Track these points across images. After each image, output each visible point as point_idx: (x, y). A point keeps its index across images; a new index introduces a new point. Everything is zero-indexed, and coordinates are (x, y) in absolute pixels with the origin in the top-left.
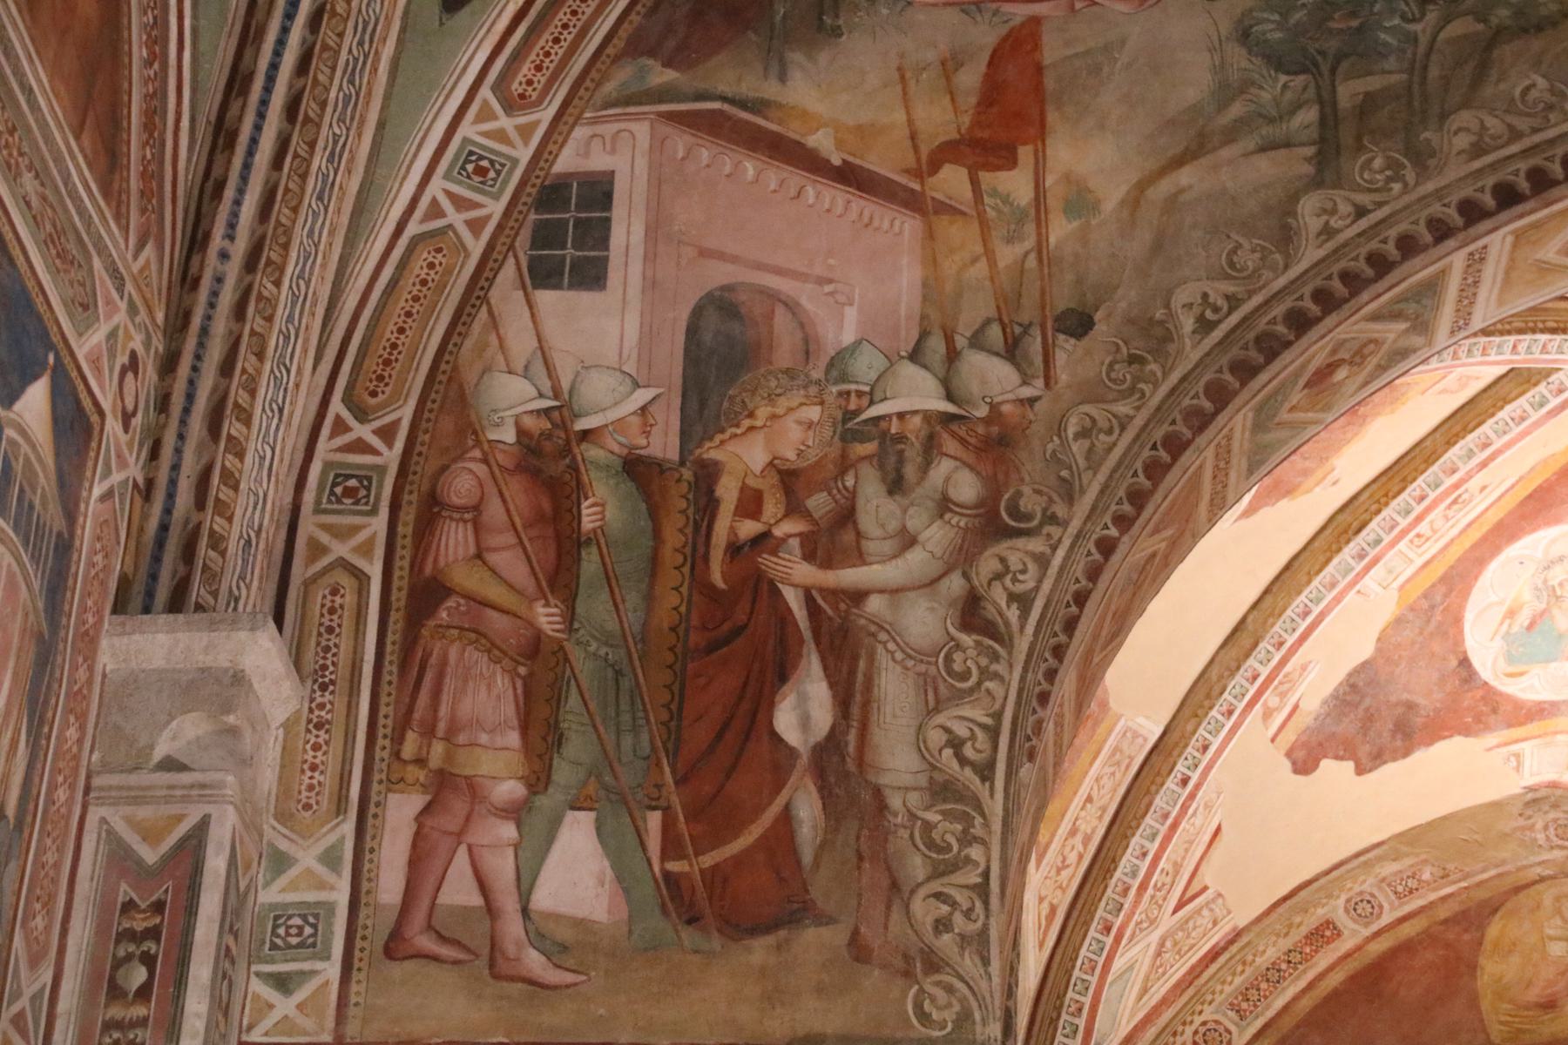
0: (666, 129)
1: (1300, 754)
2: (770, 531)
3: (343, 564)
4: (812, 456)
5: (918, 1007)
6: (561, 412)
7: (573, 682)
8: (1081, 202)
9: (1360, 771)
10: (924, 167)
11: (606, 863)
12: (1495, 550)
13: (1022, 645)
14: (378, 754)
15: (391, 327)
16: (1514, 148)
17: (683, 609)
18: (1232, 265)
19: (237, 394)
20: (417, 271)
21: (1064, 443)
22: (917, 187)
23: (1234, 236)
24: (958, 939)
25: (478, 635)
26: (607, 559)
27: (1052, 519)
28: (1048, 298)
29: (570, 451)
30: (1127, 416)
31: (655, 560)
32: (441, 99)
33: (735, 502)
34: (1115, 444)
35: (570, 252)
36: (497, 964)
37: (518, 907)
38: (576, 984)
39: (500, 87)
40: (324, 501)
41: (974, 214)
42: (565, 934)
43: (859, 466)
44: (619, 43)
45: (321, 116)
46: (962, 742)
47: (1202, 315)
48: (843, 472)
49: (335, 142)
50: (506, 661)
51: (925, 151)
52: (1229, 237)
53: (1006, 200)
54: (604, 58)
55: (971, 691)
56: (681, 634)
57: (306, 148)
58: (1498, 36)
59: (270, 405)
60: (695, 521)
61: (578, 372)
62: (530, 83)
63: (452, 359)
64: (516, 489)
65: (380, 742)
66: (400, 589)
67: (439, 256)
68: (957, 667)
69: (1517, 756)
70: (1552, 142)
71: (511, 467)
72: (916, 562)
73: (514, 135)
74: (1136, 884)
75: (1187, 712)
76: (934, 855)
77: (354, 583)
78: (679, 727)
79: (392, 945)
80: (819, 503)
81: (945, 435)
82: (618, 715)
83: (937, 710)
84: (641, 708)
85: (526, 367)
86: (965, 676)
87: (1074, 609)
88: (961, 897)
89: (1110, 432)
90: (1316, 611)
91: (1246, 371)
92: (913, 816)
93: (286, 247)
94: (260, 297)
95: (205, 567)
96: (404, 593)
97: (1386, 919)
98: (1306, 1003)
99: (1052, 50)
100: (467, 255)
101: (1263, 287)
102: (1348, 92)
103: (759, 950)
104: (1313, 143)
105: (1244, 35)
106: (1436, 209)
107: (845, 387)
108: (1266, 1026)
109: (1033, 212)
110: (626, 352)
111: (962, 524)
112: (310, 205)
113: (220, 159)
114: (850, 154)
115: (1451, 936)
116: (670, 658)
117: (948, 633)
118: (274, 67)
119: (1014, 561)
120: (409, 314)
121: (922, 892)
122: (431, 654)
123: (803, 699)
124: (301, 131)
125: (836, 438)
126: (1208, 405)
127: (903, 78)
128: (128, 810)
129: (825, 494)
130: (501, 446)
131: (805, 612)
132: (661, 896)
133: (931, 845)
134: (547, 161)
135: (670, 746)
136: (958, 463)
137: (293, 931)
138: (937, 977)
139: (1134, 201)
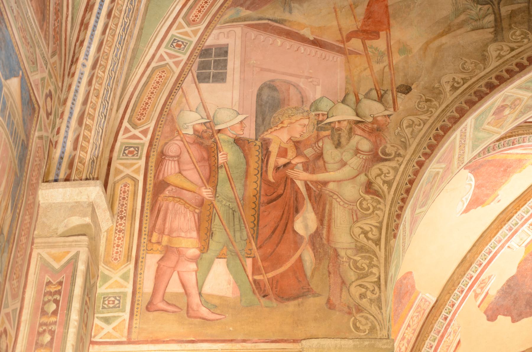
1: (490, 313)
2: (290, 162)
3: (128, 176)
4: (306, 136)
5: (355, 325)
6: (210, 124)
7: (216, 214)
8: (404, 49)
9: (514, 321)
10: (345, 39)
11: (231, 277)
13: (389, 198)
14: (142, 241)
15: (146, 97)
17: (258, 189)
18: (464, 68)
20: (155, 79)
22: (342, 46)
23: (464, 59)
24: (369, 301)
26: (229, 172)
27: (399, 155)
28: (393, 81)
29: (214, 136)
30: (426, 120)
31: (247, 172)
32: (164, 21)
33: (277, 152)
34: (422, 129)
35: (212, 71)
37: (197, 292)
38: (220, 319)
39: (185, 18)
40: (121, 155)
41: (364, 54)
42: (216, 301)
43: (324, 139)
45: (120, 15)
46: (368, 232)
47: (453, 85)
48: (318, 141)
49: (125, 25)
50: (191, 208)
51: (345, 34)
52: (462, 59)
53: (376, 49)
54: (224, 7)
55: (370, 214)
56: (258, 198)
57: (114, 26)
59: (101, 114)
60: (262, 159)
61: (216, 110)
62: (196, 16)
63: (169, 107)
64: (195, 151)
65: (143, 236)
66: (150, 184)
67: (164, 73)
68: (365, 206)
71: (192, 142)
72: (346, 171)
73: (191, 34)
76: (358, 271)
77: (133, 183)
78: (258, 229)
79: (149, 307)
80: (309, 152)
81: (356, 128)
82: (234, 225)
83: (357, 221)
84: (243, 223)
85: (197, 109)
86: (368, 209)
87: (409, 185)
88: (368, 285)
90: (494, 251)
91: (472, 104)
92: (349, 258)
93: (107, 59)
94: (97, 77)
95: (77, 169)
96: (152, 185)
101: (475, 76)
103: (291, 306)
104: (493, 27)
107: (318, 112)
109: (386, 53)
110: (234, 104)
111: (364, 158)
112: (116, 45)
114: (317, 36)
116: (254, 206)
117: (360, 195)
119: (385, 170)
120: (152, 93)
121: (354, 284)
122: (162, 206)
123: (305, 219)
124: (112, 20)
125: (315, 130)
126: (457, 115)
127: (335, 11)
128: (48, 250)
129: (311, 148)
130: (188, 135)
131: (305, 189)
132: (253, 288)
133: (357, 268)
134: (203, 41)
135: (255, 236)
136: (362, 137)
137: (111, 302)
138: (361, 314)
139: (426, 47)
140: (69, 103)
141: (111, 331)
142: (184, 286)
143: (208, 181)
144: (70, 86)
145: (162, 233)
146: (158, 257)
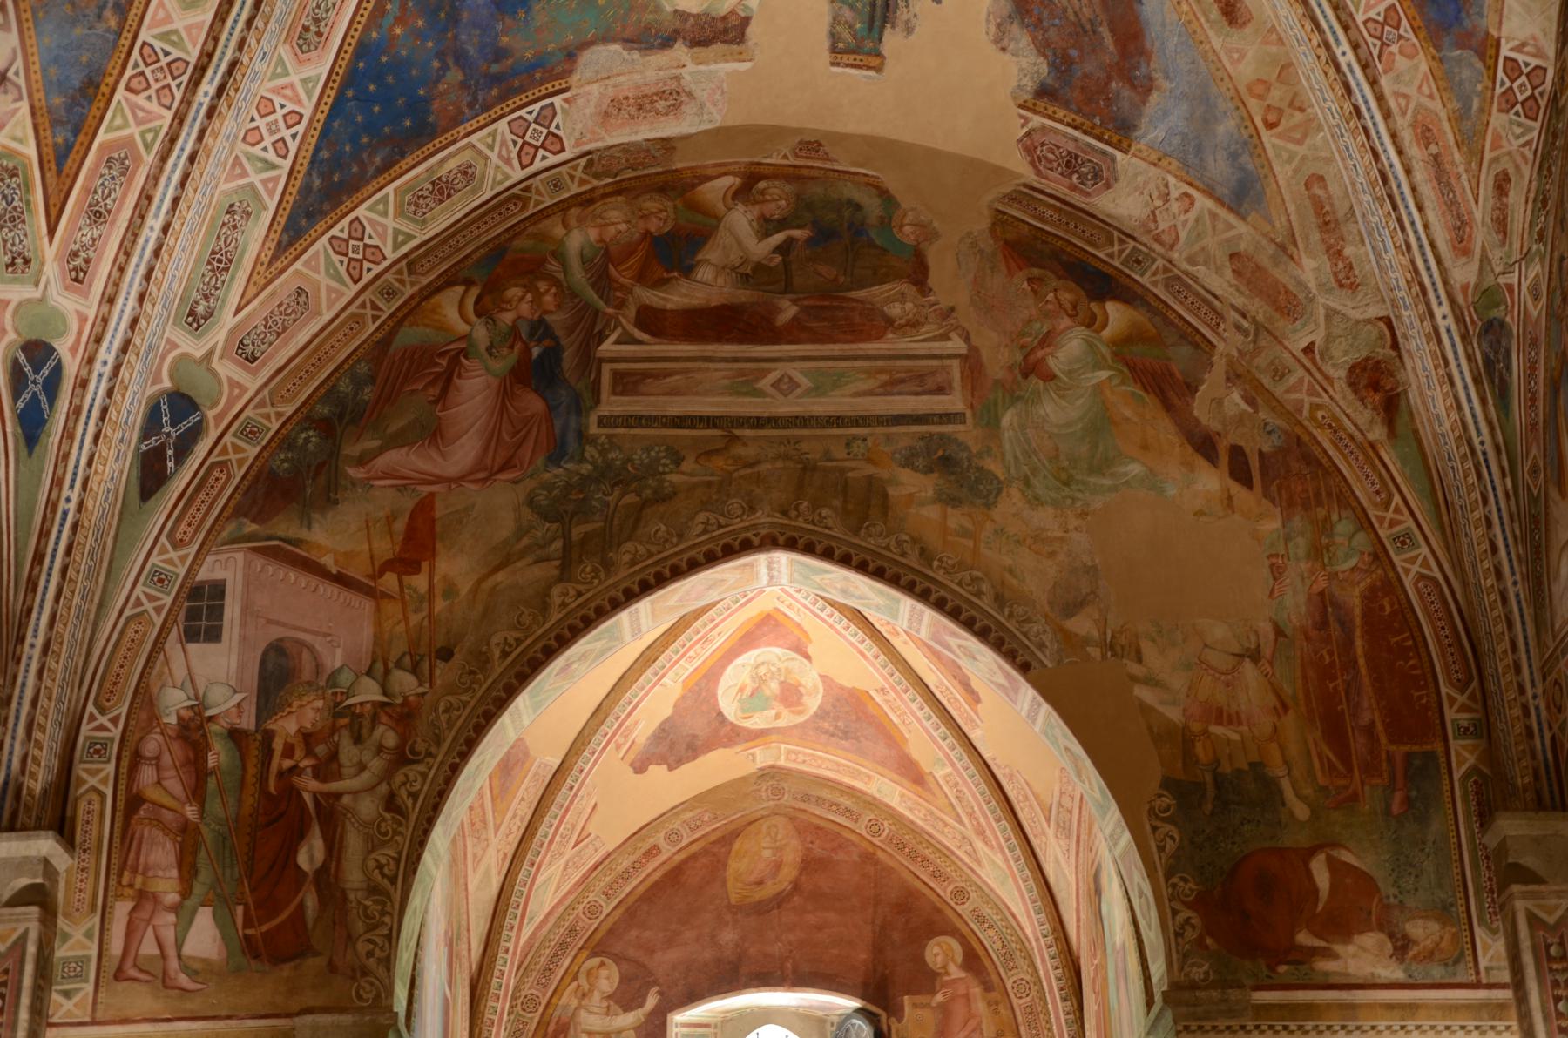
0: (252, 556)
1: (637, 764)
3: (94, 789)
5: (357, 993)
6: (199, 707)
8: (450, 591)
9: (671, 769)
11: (217, 932)
12: (730, 661)
13: (413, 817)
14: (111, 883)
15: (117, 665)
16: (650, 561)
18: (519, 622)
19: (39, 718)
21: (437, 716)
22: (372, 584)
25: (158, 822)
27: (430, 755)
35: (204, 623)
36: (166, 982)
39: (170, 536)
41: (397, 596)
42: (197, 966)
44: (229, 510)
48: (332, 734)
50: (171, 835)
53: (415, 590)
55: (389, 841)
58: (645, 504)
64: (177, 748)
65: (112, 877)
68: (383, 830)
69: (753, 755)
70: (665, 559)
73: (177, 562)
74: (547, 841)
75: (573, 751)
80: (321, 750)
81: (382, 714)
85: (182, 684)
88: (377, 940)
89: (458, 710)
93: (61, 643)
94: (49, 669)
97: (685, 842)
98: (641, 889)
99: (440, 511)
100: (154, 625)
102: (577, 532)
103: (286, 970)
105: (531, 502)
106: (613, 593)
108: (621, 902)
113: (29, 598)
115: (716, 850)
118: (55, 550)
119: (412, 775)
121: (362, 939)
123: (311, 849)
126: (504, 695)
127: (367, 526)
133: (367, 916)
139: (475, 590)
140: (14, 705)
141: (73, 1008)
142: (160, 945)
143: (194, 793)
144: (15, 677)
145: (135, 871)
146: (129, 905)
